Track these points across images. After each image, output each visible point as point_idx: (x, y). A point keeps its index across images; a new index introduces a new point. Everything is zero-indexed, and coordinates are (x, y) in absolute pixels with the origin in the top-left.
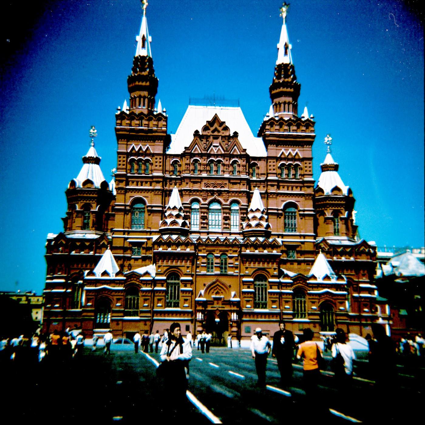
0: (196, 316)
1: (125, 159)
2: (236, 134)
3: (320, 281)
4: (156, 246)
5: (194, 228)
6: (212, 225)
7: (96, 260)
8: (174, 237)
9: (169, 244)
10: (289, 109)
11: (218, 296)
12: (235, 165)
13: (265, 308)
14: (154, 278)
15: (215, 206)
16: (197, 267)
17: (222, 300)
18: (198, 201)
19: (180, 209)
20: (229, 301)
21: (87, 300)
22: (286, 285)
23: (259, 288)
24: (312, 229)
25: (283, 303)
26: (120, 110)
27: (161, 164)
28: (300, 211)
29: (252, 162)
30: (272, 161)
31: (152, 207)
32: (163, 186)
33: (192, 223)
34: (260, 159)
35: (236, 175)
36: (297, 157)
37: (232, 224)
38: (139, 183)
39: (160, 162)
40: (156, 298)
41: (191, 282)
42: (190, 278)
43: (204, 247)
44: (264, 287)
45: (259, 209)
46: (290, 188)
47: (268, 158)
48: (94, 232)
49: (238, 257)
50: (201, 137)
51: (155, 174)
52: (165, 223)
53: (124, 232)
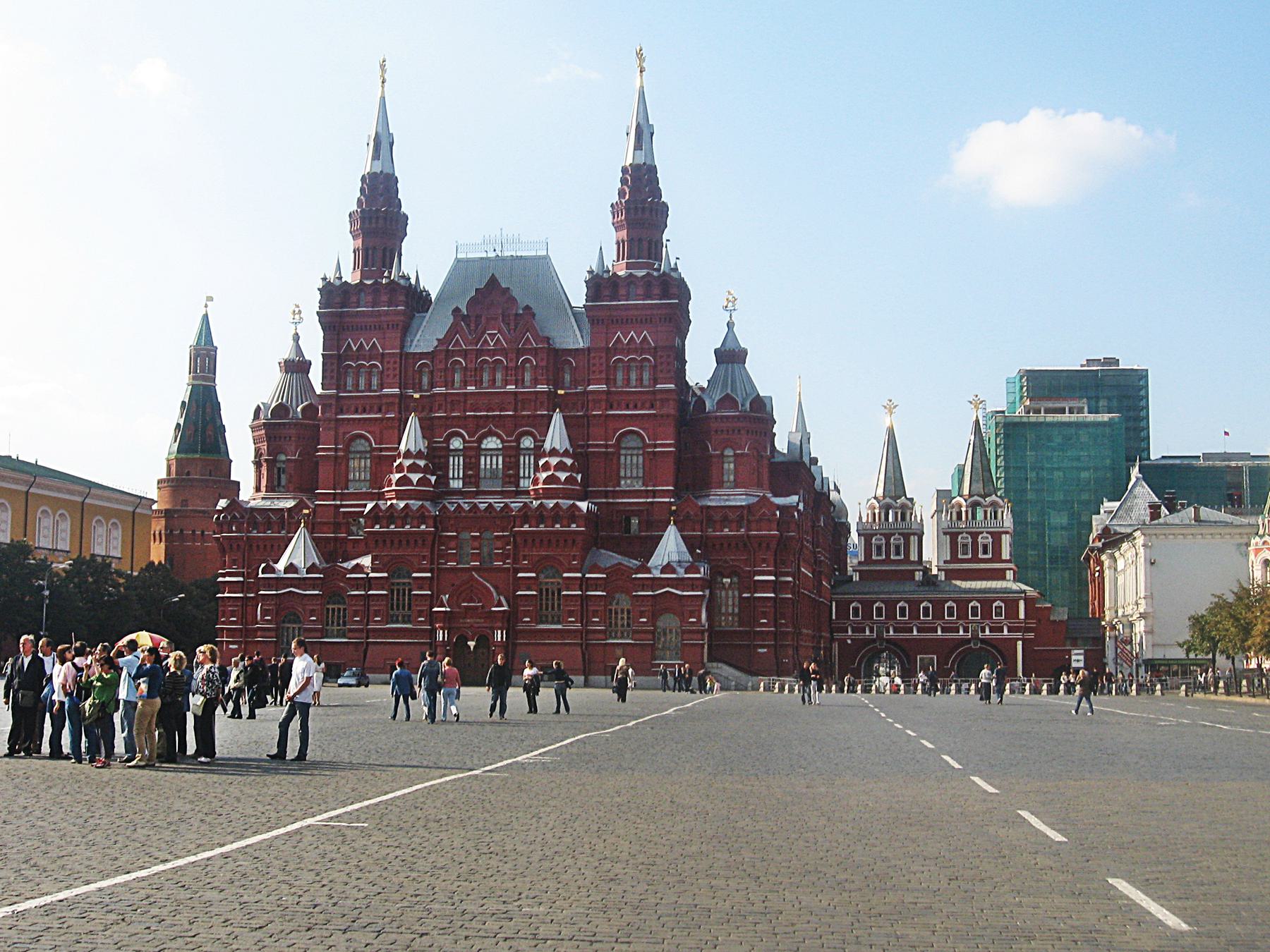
1: (335, 367)
2: (527, 308)
5: (456, 484)
9: (392, 515)
15: (492, 443)
16: (440, 557)
19: (419, 455)
21: (264, 613)
22: (595, 584)
23: (547, 590)
24: (671, 479)
28: (649, 446)
29: (556, 359)
31: (381, 450)
39: (395, 369)
44: (549, 586)
45: (558, 447)
47: (589, 349)
50: (464, 318)
53: (334, 496)
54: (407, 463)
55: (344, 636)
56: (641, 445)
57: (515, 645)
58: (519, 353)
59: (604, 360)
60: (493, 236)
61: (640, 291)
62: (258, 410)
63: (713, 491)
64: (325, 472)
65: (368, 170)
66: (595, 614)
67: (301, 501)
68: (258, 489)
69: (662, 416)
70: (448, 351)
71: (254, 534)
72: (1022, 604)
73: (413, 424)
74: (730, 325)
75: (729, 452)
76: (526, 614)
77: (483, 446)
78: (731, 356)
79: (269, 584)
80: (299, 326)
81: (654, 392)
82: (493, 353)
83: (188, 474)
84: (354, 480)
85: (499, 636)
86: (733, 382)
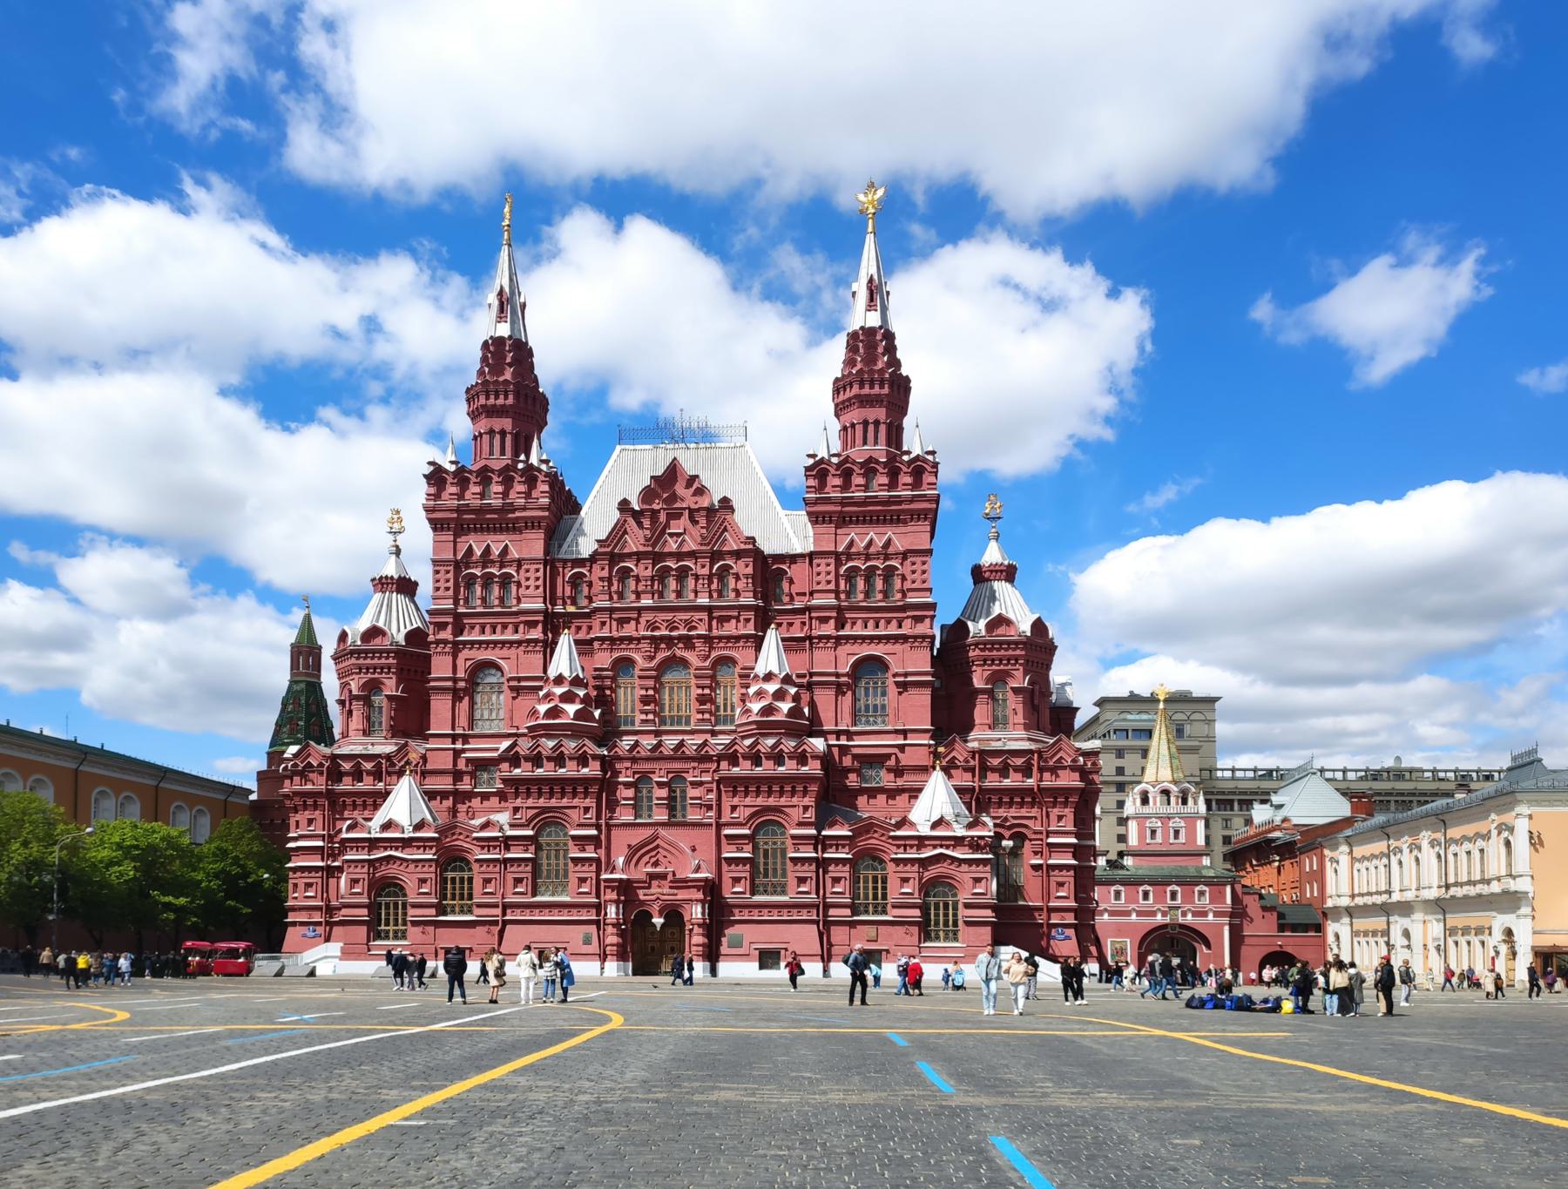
1: (451, 575)
3: (925, 830)
10: (876, 438)
11: (658, 870)
17: (670, 877)
20: (685, 881)
22: (837, 841)
25: (829, 882)
27: (540, 582)
30: (823, 562)
32: (545, 633)
34: (793, 559)
35: (730, 599)
38: (488, 629)
40: (510, 877)
41: (595, 841)
43: (628, 764)
46: (871, 624)
51: (523, 606)
55: (470, 912)
58: (715, 556)
59: (832, 568)
61: (885, 480)
69: (915, 637)
73: (565, 642)
81: (904, 608)
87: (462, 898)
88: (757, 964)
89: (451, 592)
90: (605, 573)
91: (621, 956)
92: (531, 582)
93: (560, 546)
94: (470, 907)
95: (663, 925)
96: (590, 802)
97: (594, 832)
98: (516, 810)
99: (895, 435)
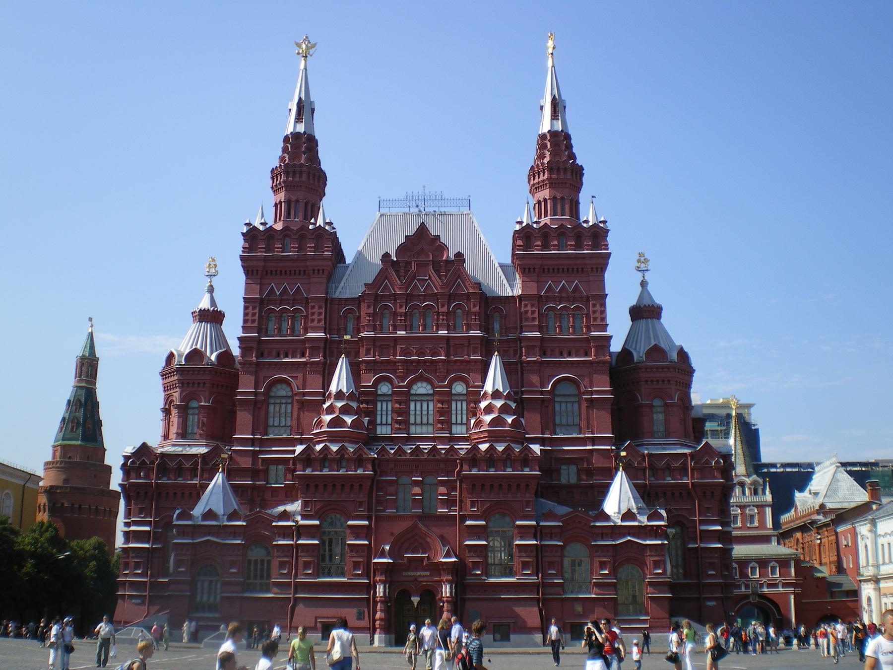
0: (375, 593)
1: (257, 311)
2: (459, 256)
4: (299, 466)
6: (415, 424)
7: (197, 493)
8: (334, 448)
12: (459, 311)
13: (511, 575)
14: (297, 522)
15: (422, 388)
16: (379, 503)
17: (425, 562)
18: (389, 380)
19: (351, 397)
21: (179, 563)
22: (549, 533)
26: (247, 224)
27: (323, 317)
29: (490, 305)
31: (304, 394)
33: (379, 421)
36: (577, 295)
37: (454, 421)
39: (320, 314)
42: (366, 523)
47: (520, 297)
48: (203, 442)
49: (455, 481)
51: (310, 335)
52: (320, 423)
53: (253, 442)
54: (339, 404)
56: (576, 392)
57: (464, 600)
58: (451, 297)
60: (415, 193)
62: (171, 356)
63: (646, 441)
64: (244, 418)
65: (290, 129)
66: (551, 565)
67: (217, 447)
68: (166, 437)
70: (377, 296)
71: (164, 481)
72: (792, 563)
74: (644, 284)
75: (657, 402)
76: (476, 565)
77: (413, 392)
78: (645, 312)
79: (184, 531)
80: (214, 279)
81: (588, 340)
82: (425, 298)
83: (70, 458)
84: (273, 426)
85: (446, 591)
86: (656, 336)
87: (262, 577)
88: (491, 637)
89: (256, 324)
90: (371, 310)
91: (386, 630)
92: (316, 317)
93: (336, 288)
94: (268, 585)
95: (419, 603)
96: (363, 497)
97: (366, 523)
98: (305, 504)
99: (575, 208)
